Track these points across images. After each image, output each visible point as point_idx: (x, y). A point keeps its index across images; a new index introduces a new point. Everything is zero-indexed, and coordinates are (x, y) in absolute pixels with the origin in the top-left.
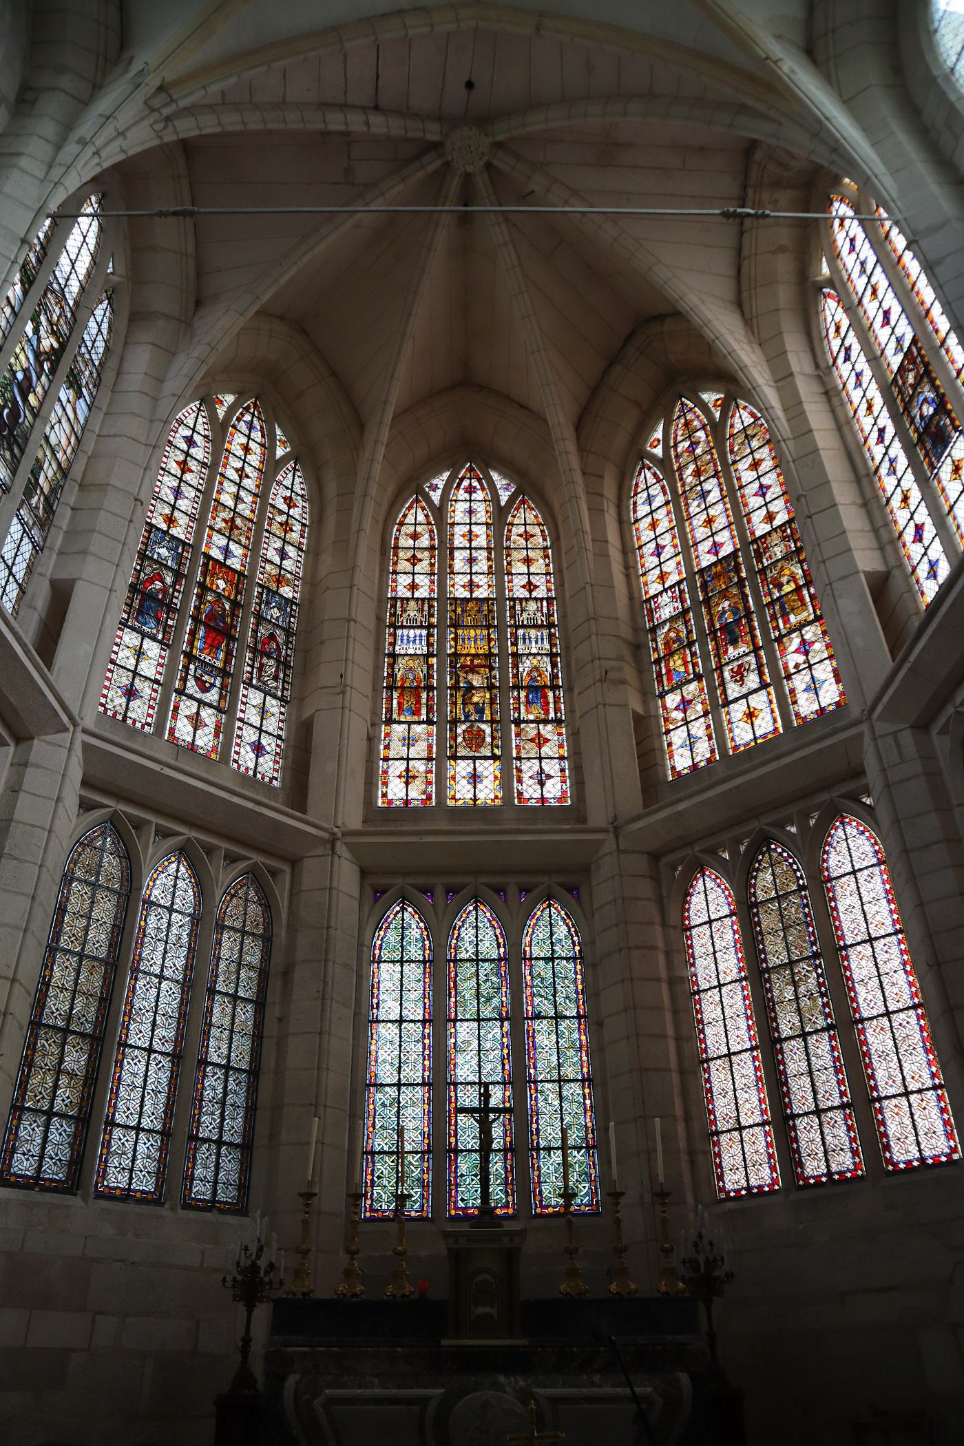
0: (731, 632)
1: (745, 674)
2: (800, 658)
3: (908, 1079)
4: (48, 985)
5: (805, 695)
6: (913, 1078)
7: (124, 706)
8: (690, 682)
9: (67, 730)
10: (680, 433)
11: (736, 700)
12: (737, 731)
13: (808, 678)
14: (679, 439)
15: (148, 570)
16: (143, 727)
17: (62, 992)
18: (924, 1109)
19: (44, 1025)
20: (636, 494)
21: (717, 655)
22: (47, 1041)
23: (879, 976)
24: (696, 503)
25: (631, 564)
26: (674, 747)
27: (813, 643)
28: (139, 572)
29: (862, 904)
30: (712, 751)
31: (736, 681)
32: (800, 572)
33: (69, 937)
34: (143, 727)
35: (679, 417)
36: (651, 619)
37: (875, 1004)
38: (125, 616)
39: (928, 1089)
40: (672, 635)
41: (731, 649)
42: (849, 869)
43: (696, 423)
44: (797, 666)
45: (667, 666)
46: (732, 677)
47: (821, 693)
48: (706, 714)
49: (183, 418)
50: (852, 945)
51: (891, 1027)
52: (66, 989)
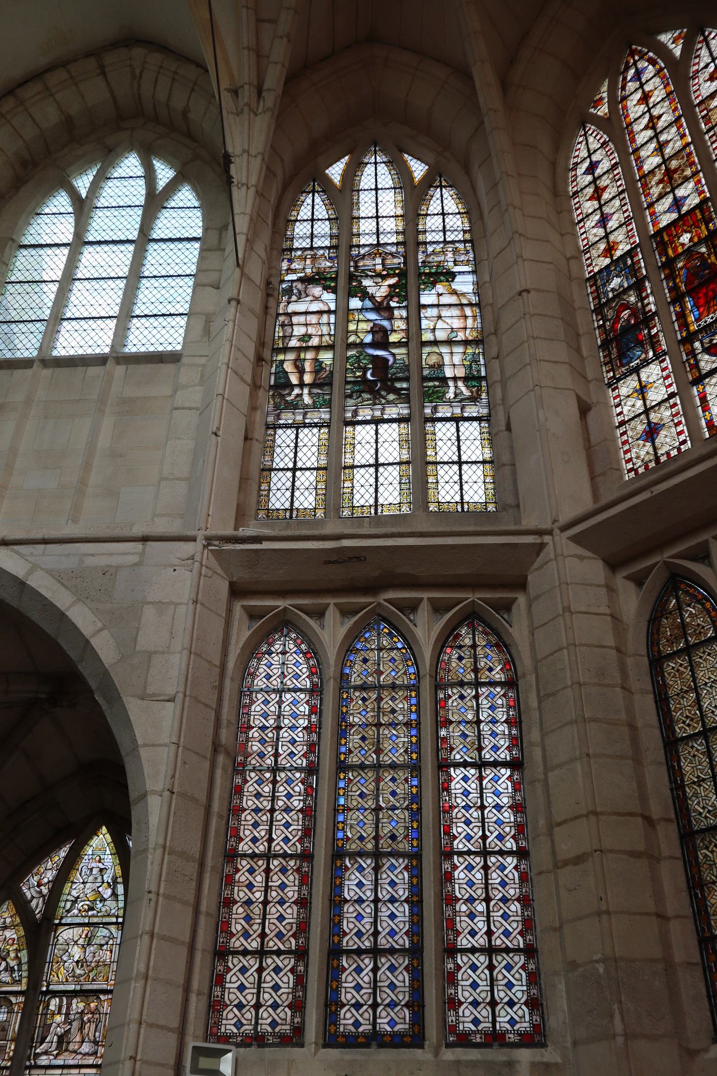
4: (682, 787)
7: (651, 451)
9: (542, 546)
15: (610, 314)
16: (679, 449)
17: (700, 786)
19: (698, 832)
22: (707, 848)
28: (604, 325)
33: (684, 722)
34: (679, 449)
38: (611, 374)
49: (576, 160)
52: (704, 780)
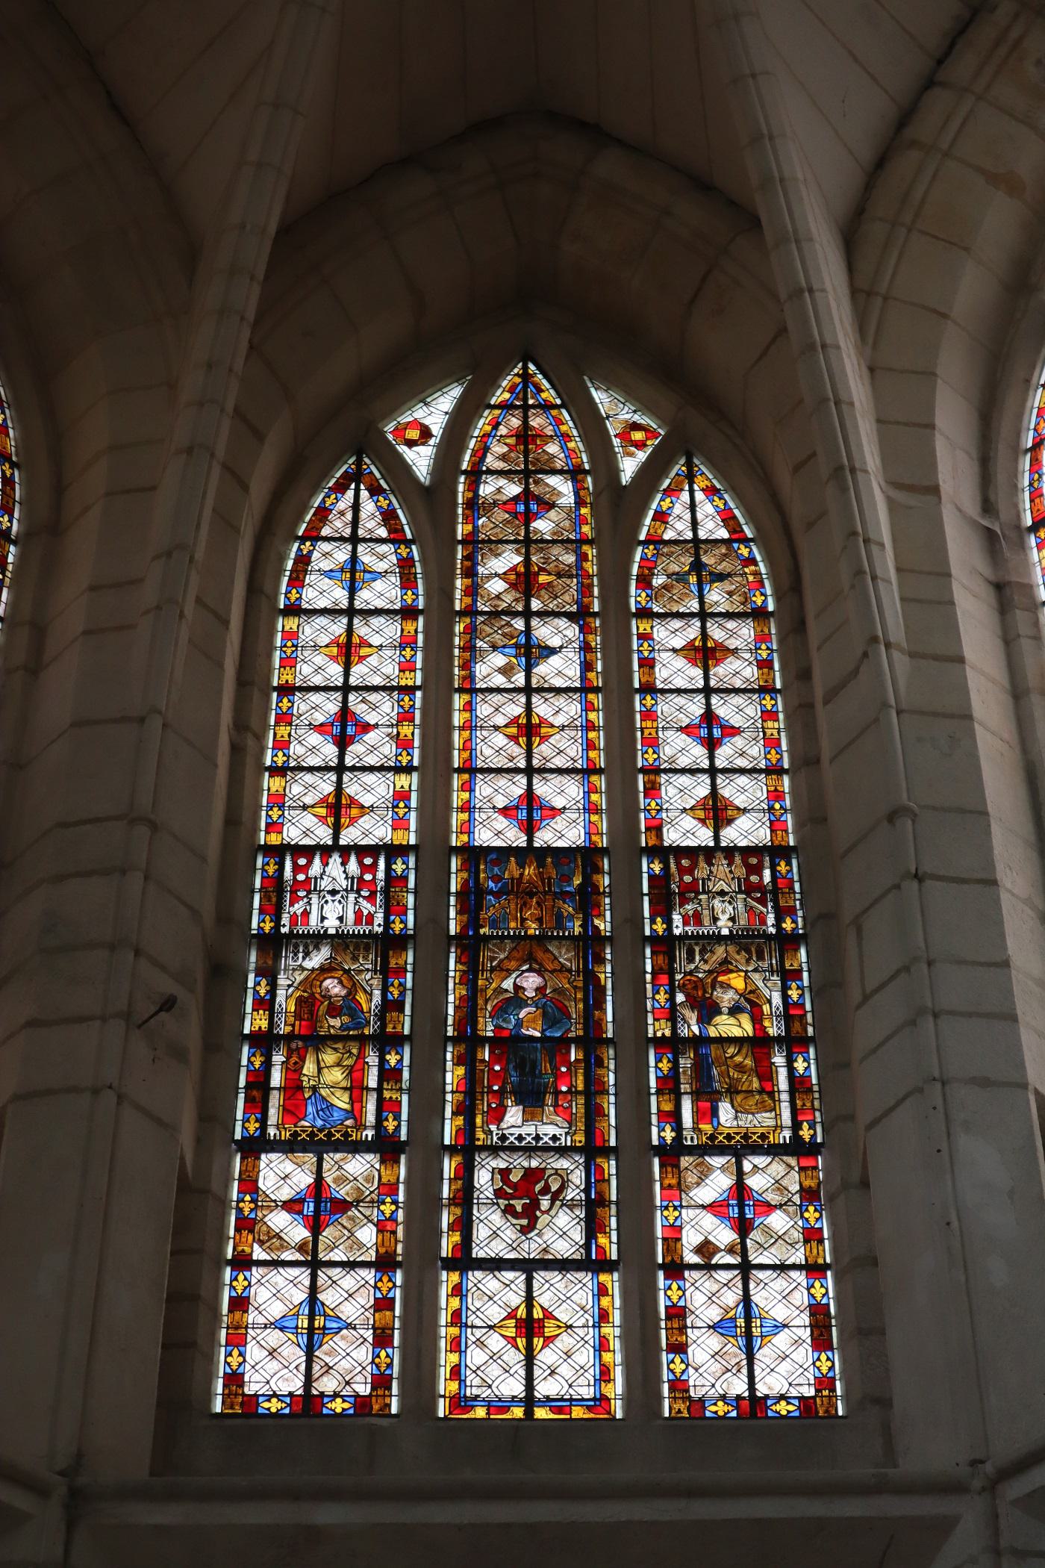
0: (527, 1068)
1: (545, 1204)
2: (725, 1236)
5: (714, 1342)
8: (357, 1148)
10: (499, 449)
11: (495, 1265)
12: (475, 1357)
13: (731, 1297)
14: (491, 462)
20: (313, 536)
21: (466, 1110)
24: (499, 660)
25: (254, 723)
26: (252, 1317)
27: (769, 1208)
30: (381, 1382)
31: (509, 1211)
32: (777, 999)
35: (505, 406)
36: (274, 910)
40: (333, 986)
41: (514, 1115)
43: (553, 448)
44: (706, 1249)
45: (293, 1072)
46: (499, 1193)
47: (764, 1356)
48: (384, 1263)
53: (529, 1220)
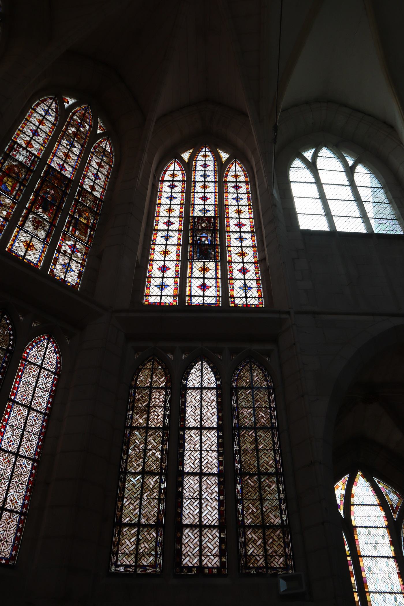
1: (40, 227)
2: (69, 251)
3: (8, 501)
5: (61, 267)
6: (11, 501)
12: (16, 244)
13: (66, 261)
18: (8, 523)
23: (24, 430)
27: (78, 252)
29: (36, 386)
31: (33, 224)
32: (92, 221)
37: (13, 444)
39: (17, 512)
41: (40, 210)
42: (39, 363)
43: (88, 120)
44: (65, 251)
46: (32, 220)
47: (69, 274)
50: (18, 403)
51: (15, 464)
53: (36, 228)
